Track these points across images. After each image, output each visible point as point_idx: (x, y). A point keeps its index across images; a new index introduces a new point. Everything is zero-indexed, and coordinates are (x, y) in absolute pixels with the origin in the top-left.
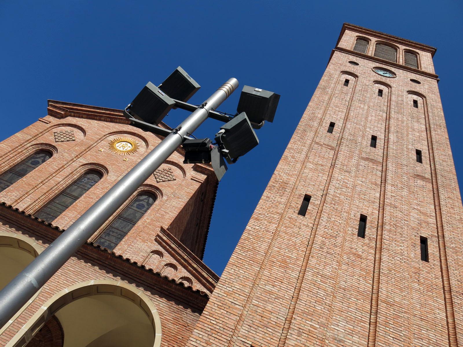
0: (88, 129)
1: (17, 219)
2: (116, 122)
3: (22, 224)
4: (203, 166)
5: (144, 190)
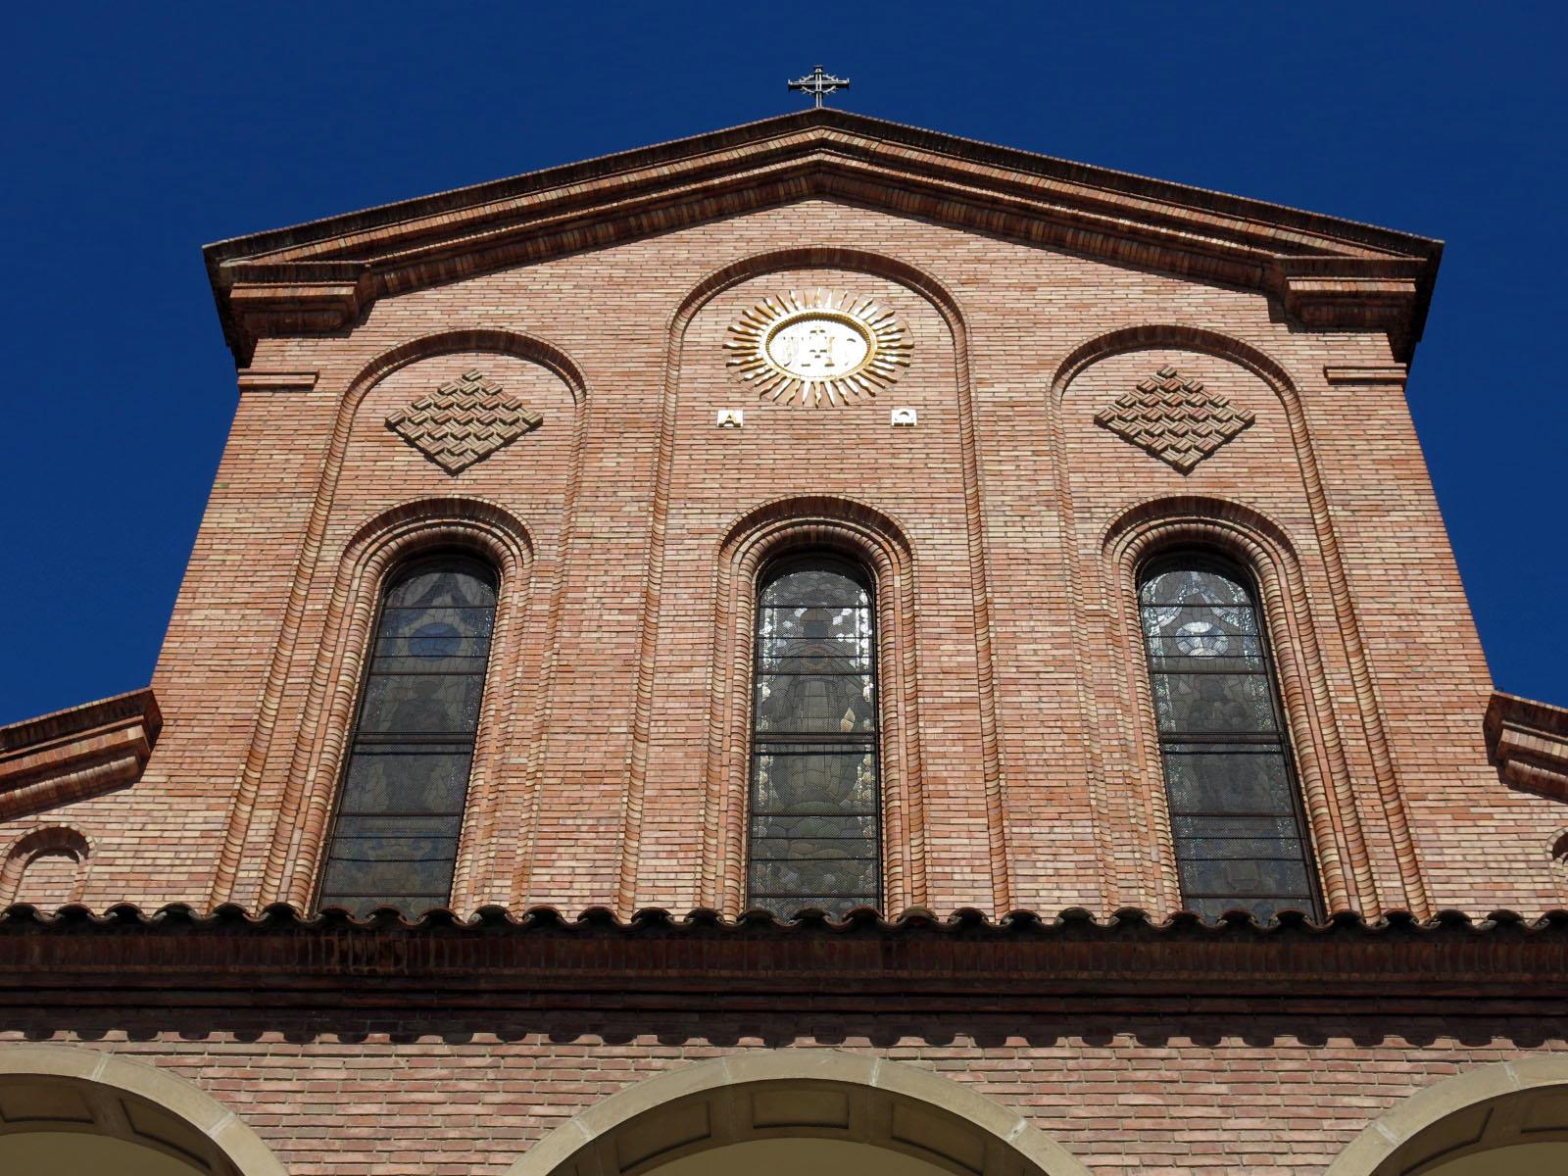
0: (544, 327)
1: (1417, 976)
2: (655, 231)
3: (1475, 993)
4: (1339, 288)
5: (1148, 545)
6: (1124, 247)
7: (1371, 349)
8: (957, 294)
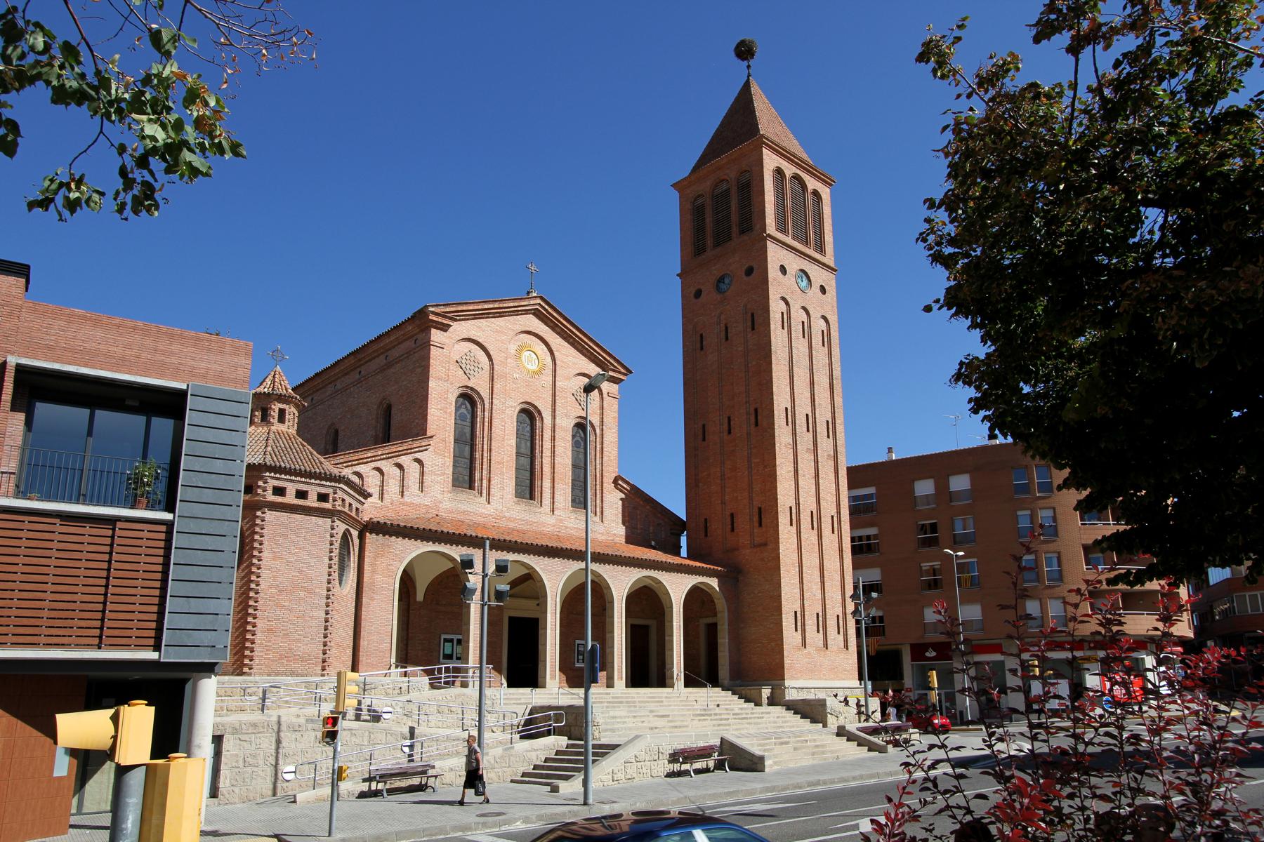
6: (585, 351)
8: (556, 354)
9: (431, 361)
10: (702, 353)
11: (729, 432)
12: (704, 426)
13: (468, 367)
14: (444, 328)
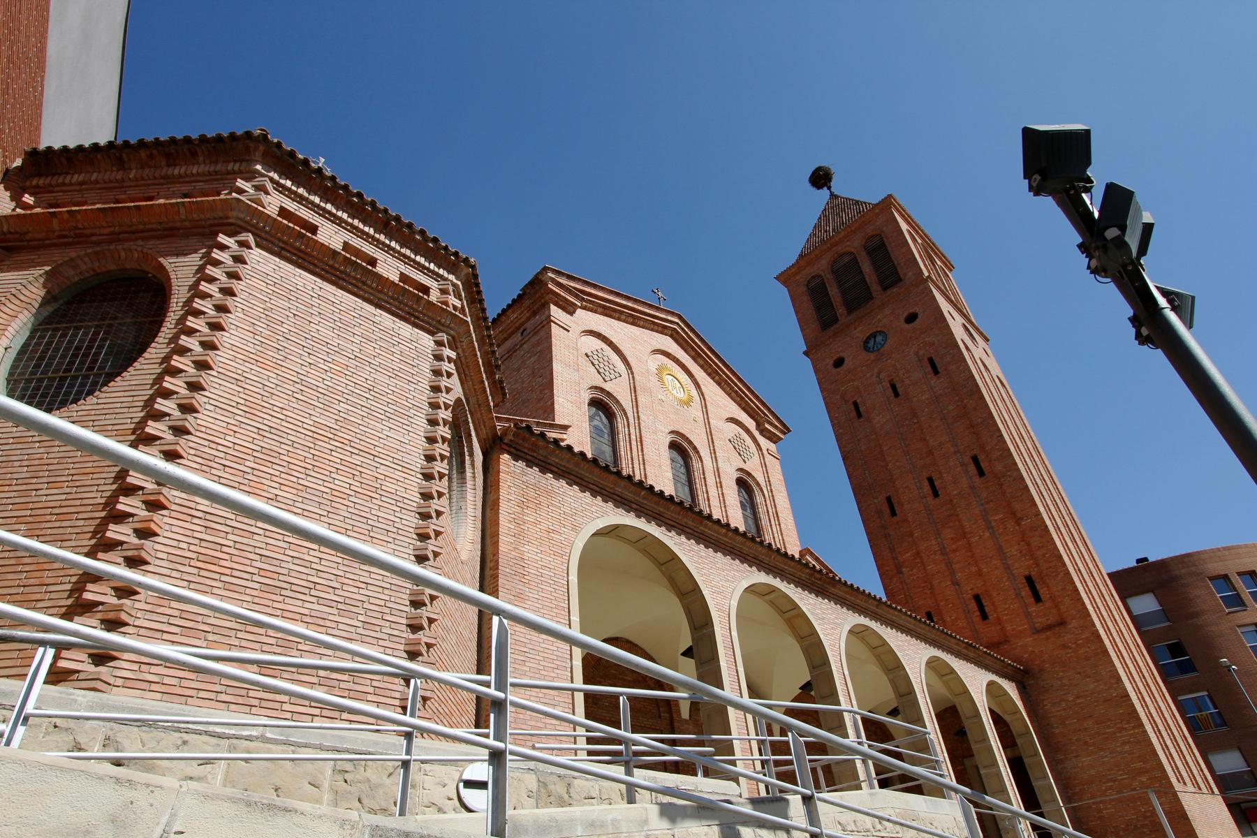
2: (639, 326)
7: (772, 447)
8: (703, 387)
9: (553, 340)
10: (861, 420)
11: (936, 494)
12: (889, 499)
13: (602, 365)
14: (569, 309)
